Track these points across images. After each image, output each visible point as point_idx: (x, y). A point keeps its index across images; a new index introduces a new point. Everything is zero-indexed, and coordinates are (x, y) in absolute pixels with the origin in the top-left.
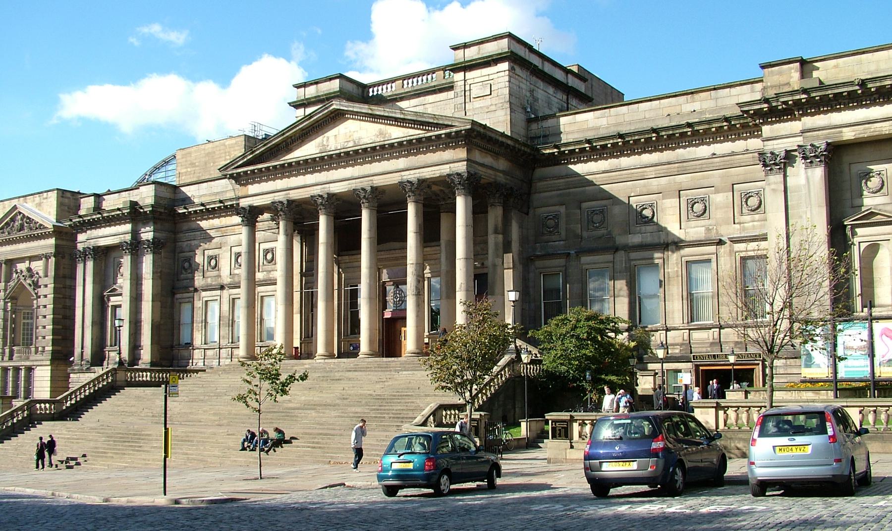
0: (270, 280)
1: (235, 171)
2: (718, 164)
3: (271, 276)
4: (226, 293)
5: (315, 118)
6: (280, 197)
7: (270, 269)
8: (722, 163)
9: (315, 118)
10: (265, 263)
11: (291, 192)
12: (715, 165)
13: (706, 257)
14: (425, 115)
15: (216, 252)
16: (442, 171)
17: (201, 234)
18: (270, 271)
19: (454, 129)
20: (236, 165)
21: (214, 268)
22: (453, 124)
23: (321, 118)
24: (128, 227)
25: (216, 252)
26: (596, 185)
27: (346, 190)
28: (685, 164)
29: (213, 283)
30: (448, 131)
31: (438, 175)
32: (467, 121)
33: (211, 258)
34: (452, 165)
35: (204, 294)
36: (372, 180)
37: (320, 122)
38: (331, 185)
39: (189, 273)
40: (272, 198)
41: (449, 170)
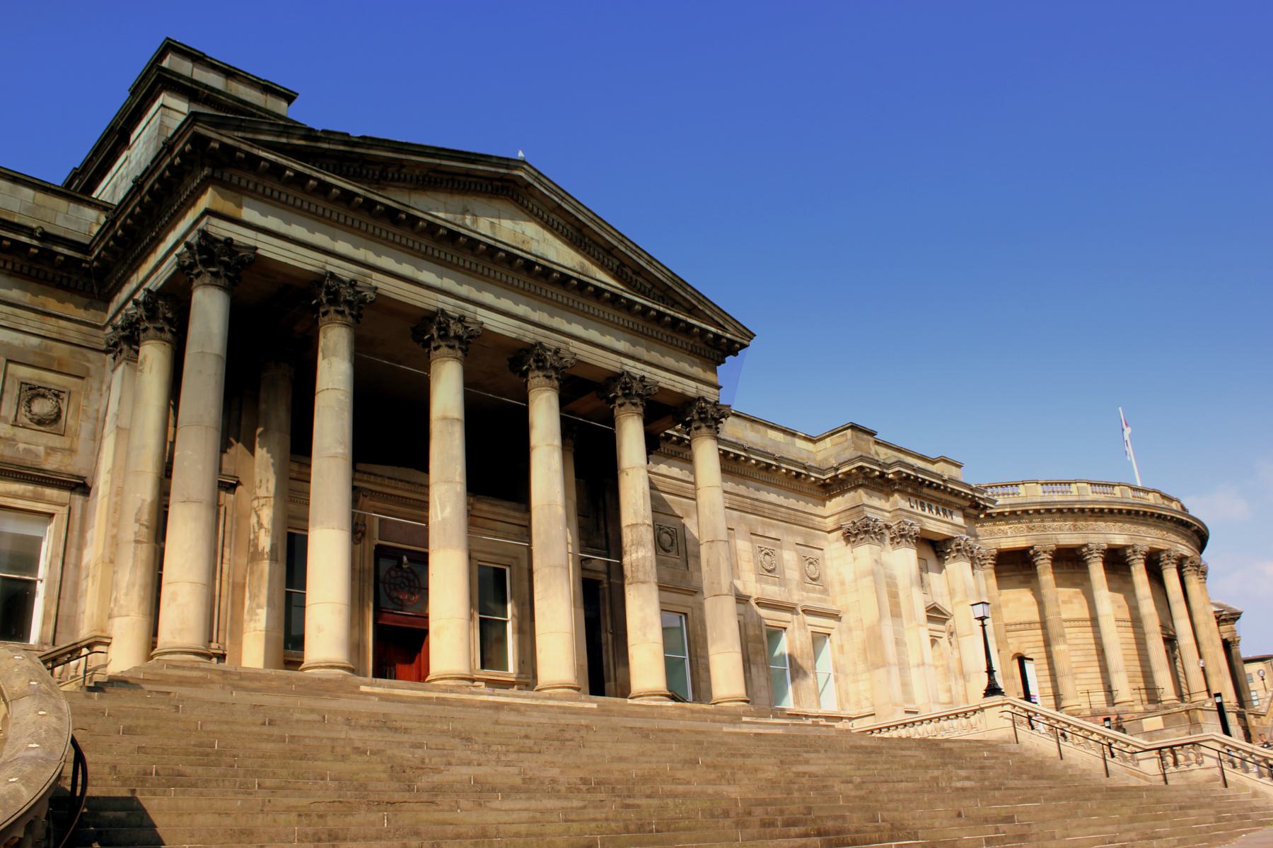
1: (245, 147)
2: (783, 515)
5: (480, 167)
6: (345, 273)
8: (787, 516)
9: (480, 167)
11: (376, 275)
12: (779, 514)
13: (783, 624)
14: (689, 289)
16: (686, 388)
19: (728, 336)
20: (250, 136)
22: (726, 326)
23: (478, 173)
26: (657, 490)
27: (514, 336)
28: (756, 503)
30: (720, 332)
31: (679, 391)
32: (748, 334)
34: (700, 386)
36: (564, 342)
37: (470, 179)
40: (321, 264)
41: (694, 390)
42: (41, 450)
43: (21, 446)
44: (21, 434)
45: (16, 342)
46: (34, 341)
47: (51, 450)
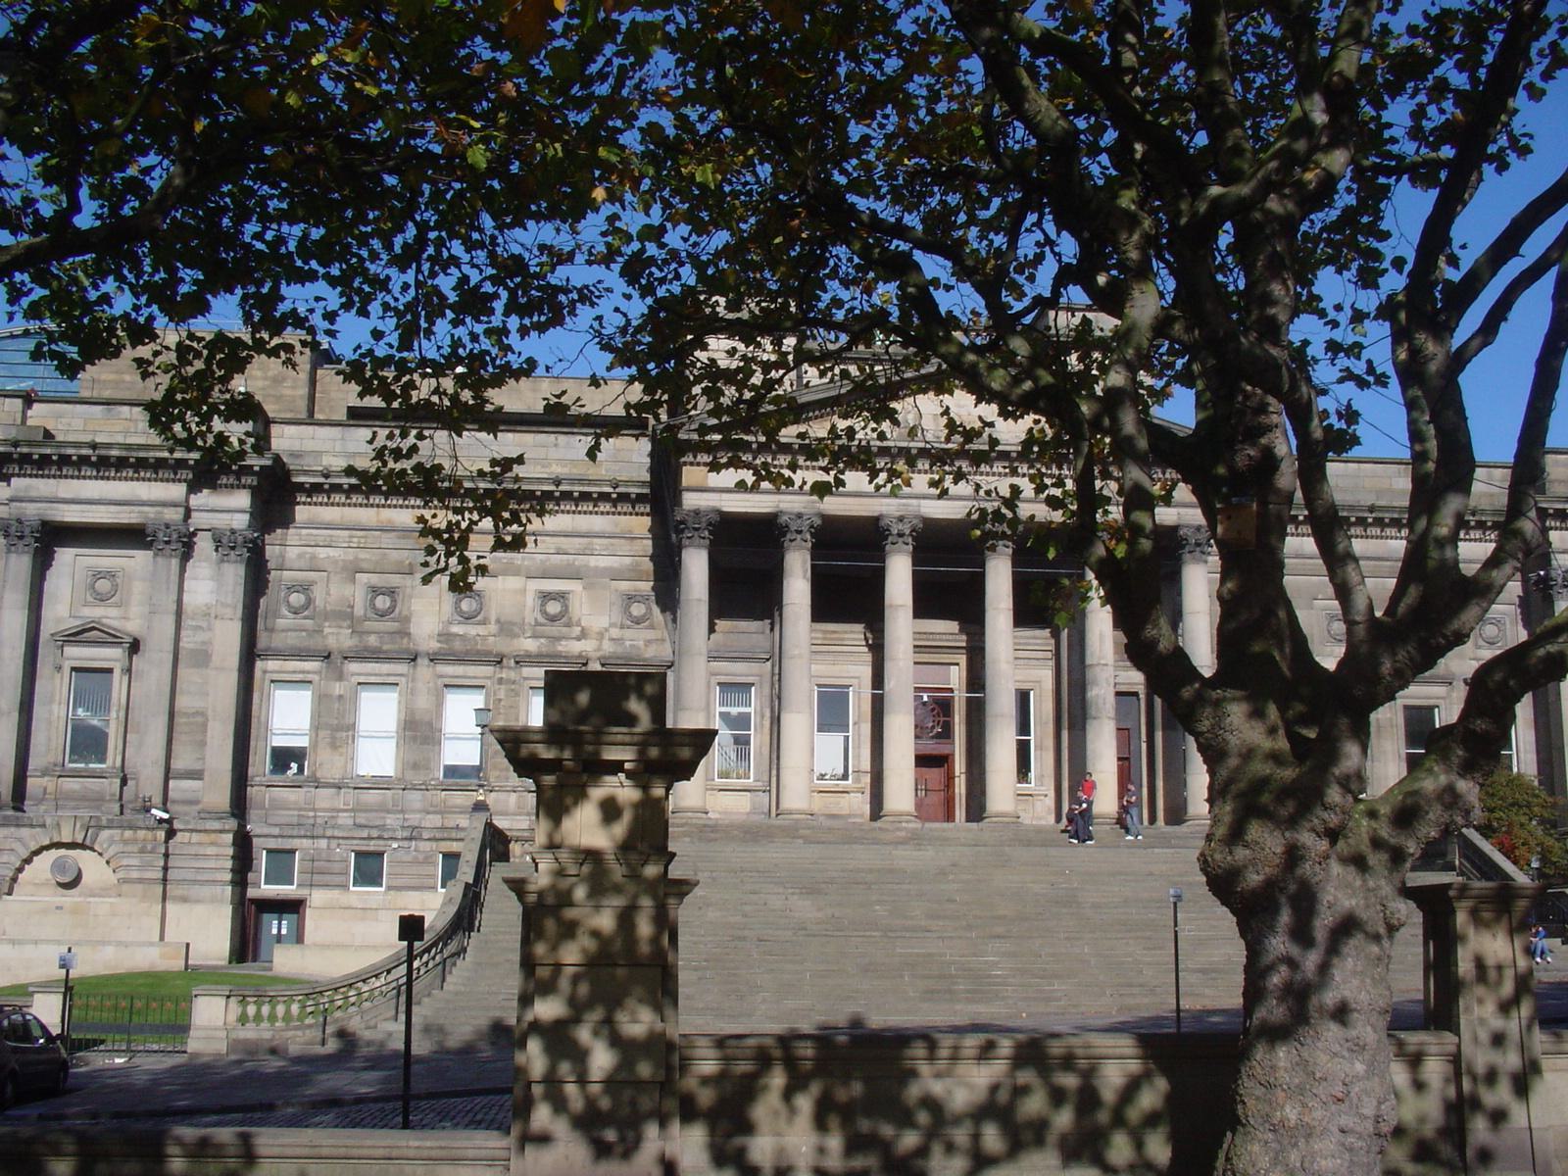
0: (561, 657)
3: (560, 648)
4: (424, 668)
7: (557, 634)
10: (541, 620)
13: (1431, 702)
15: (395, 580)
17: (351, 537)
18: (558, 639)
21: (382, 615)
24: (177, 491)
25: (395, 580)
29: (385, 647)
33: (375, 591)
35: (353, 667)
38: (923, 502)
39: (305, 618)
42: (641, 643)
43: (628, 643)
44: (628, 633)
45: (616, 565)
46: (628, 560)
47: (648, 643)
